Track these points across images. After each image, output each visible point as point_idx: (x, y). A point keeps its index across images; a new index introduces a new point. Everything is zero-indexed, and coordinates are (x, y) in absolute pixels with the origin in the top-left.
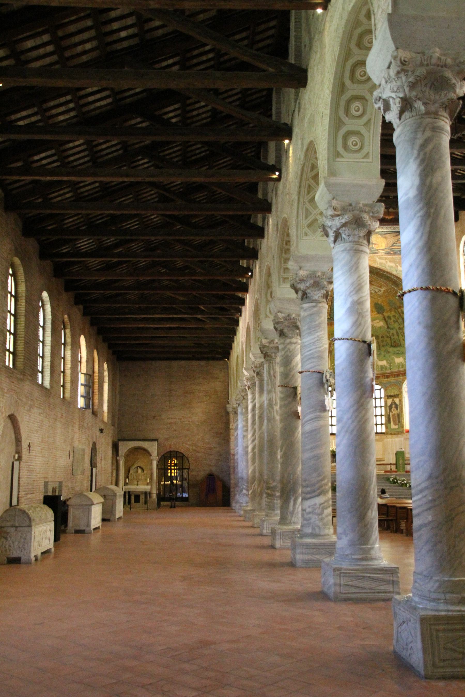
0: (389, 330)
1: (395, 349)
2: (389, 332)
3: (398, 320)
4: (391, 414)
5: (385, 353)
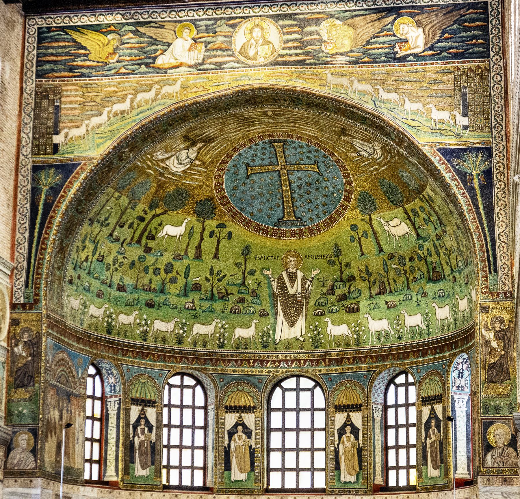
1: (437, 286)
2: (421, 247)
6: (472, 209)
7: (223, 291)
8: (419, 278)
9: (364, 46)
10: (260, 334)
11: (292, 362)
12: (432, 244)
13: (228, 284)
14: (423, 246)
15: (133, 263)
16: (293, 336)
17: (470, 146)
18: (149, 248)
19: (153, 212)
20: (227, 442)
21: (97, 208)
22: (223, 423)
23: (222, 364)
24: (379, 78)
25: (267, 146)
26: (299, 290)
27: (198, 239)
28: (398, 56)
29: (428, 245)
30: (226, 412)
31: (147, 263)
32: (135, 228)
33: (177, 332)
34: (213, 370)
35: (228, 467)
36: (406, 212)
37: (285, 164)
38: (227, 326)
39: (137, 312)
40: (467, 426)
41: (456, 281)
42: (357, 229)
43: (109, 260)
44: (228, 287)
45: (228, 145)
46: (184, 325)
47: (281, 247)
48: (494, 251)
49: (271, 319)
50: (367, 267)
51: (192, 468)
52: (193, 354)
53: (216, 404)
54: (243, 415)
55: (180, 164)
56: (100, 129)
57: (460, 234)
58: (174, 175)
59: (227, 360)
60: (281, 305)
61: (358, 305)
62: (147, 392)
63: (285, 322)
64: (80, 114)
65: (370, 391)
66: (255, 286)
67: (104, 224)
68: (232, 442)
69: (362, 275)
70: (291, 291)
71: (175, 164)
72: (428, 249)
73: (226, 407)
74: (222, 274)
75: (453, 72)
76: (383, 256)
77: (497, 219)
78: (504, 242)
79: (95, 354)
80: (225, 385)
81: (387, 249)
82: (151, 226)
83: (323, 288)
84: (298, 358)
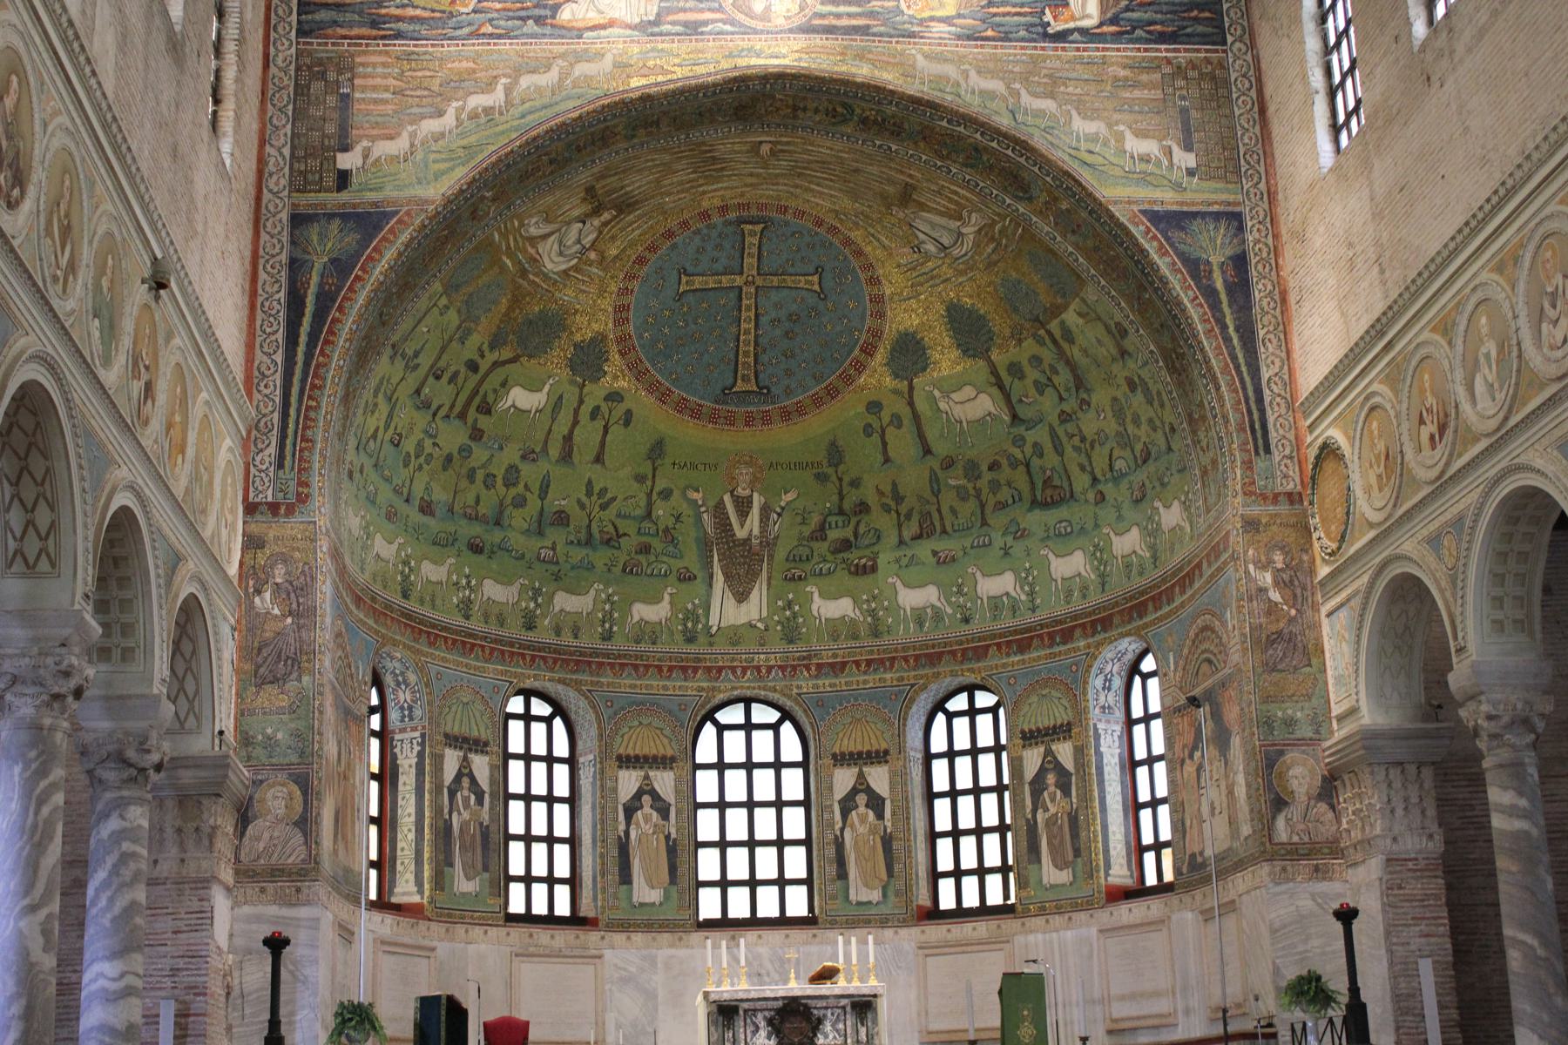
0: (1021, 430)
1: (1052, 516)
2: (1019, 441)
3: (1056, 380)
4: (1040, 816)
5: (1009, 539)
7: (612, 530)
9: (983, 7)
11: (744, 670)
13: (619, 516)
14: (1023, 439)
15: (449, 459)
18: (480, 430)
20: (622, 827)
22: (615, 790)
23: (609, 672)
24: (1017, 69)
26: (756, 531)
28: (1051, 31)
29: (1039, 435)
30: (620, 767)
32: (460, 386)
33: (524, 605)
35: (626, 878)
36: (994, 372)
38: (616, 598)
39: (453, 561)
40: (1122, 783)
41: (1104, 499)
44: (618, 522)
46: (537, 592)
48: (1262, 411)
49: (699, 585)
50: (894, 485)
51: (551, 880)
52: (555, 651)
53: (601, 752)
54: (651, 774)
55: (561, 254)
57: (1138, 399)
58: (546, 277)
61: (874, 560)
62: (473, 721)
63: (728, 594)
65: (904, 725)
66: (671, 522)
68: (632, 827)
69: (884, 500)
70: (741, 534)
72: (1035, 445)
73: (619, 758)
74: (609, 495)
77: (1262, 349)
78: (1279, 395)
80: (615, 714)
81: (941, 448)
82: (486, 387)
84: (755, 663)
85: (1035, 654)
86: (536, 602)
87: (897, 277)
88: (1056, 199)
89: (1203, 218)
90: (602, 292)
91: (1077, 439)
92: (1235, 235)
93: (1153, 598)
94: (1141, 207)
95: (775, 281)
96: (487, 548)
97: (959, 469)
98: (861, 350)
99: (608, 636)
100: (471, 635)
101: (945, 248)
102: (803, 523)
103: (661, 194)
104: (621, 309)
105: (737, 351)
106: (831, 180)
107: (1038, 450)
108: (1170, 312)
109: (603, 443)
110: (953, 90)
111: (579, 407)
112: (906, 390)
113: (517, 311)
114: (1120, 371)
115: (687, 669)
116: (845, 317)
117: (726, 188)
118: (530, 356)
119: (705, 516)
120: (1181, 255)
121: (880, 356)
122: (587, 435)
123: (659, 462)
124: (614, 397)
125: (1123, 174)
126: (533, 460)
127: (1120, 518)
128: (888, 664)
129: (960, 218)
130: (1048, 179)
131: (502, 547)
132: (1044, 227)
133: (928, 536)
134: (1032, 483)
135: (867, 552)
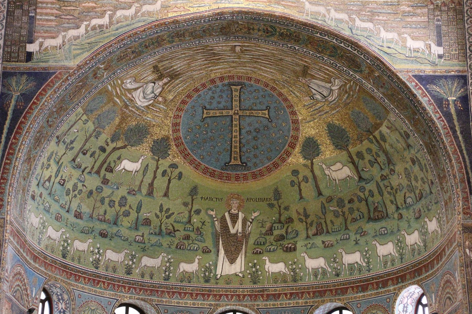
0: (363, 184)
1: (378, 225)
2: (362, 189)
3: (379, 159)
5: (358, 236)
6: (449, 132)
7: (171, 228)
8: (359, 218)
10: (203, 269)
11: (232, 296)
12: (375, 185)
13: (175, 221)
14: (364, 188)
15: (91, 193)
16: (233, 272)
17: (445, 74)
19: (114, 145)
21: (64, 127)
23: (167, 295)
24: (355, 8)
25: (226, 88)
26: (240, 230)
27: (152, 175)
29: (371, 186)
31: (104, 194)
33: (126, 262)
34: (158, 301)
37: (238, 109)
38: (172, 260)
39: (91, 241)
41: (402, 217)
42: (298, 174)
43: (69, 185)
44: (175, 225)
45: (191, 83)
46: (133, 257)
47: (225, 190)
49: (212, 256)
50: (305, 209)
52: (141, 285)
55: (144, 98)
56: (77, 41)
57: (416, 168)
58: (138, 109)
59: (172, 292)
60: (222, 244)
61: (295, 244)
63: (226, 259)
64: (56, 26)
66: (200, 225)
67: (69, 147)
70: (233, 231)
71: (141, 98)
72: (370, 191)
74: (171, 212)
75: (427, 6)
76: (321, 200)
79: (49, 276)
81: (326, 192)
82: (110, 159)
83: (262, 229)
84: (238, 293)
85: (369, 293)
86: (133, 261)
87: (304, 111)
88: (373, 71)
89: (445, 79)
90: (166, 117)
91: (389, 188)
92: (462, 87)
93: (424, 266)
94: (414, 74)
95: (248, 113)
96: (110, 235)
97: (335, 202)
98: (289, 146)
99: (167, 278)
100: (98, 277)
101: (326, 97)
102: (262, 227)
103: (191, 70)
104: (175, 125)
105: (231, 146)
106: (271, 65)
107: (371, 194)
108: (427, 125)
109: (168, 188)
110: (322, 19)
111: (156, 170)
112: (310, 165)
113: (124, 124)
114: (408, 155)
115: (205, 294)
116: (281, 130)
117: (222, 68)
118: (132, 146)
119: (216, 222)
120: (433, 97)
121: (298, 149)
122: (160, 183)
123: (195, 197)
124: (174, 166)
125: (405, 58)
126: (134, 194)
127: (409, 226)
128: (300, 295)
129: (330, 82)
130: (368, 61)
131: (117, 235)
132: (368, 86)
133: (320, 234)
134: (369, 209)
135: (292, 241)
